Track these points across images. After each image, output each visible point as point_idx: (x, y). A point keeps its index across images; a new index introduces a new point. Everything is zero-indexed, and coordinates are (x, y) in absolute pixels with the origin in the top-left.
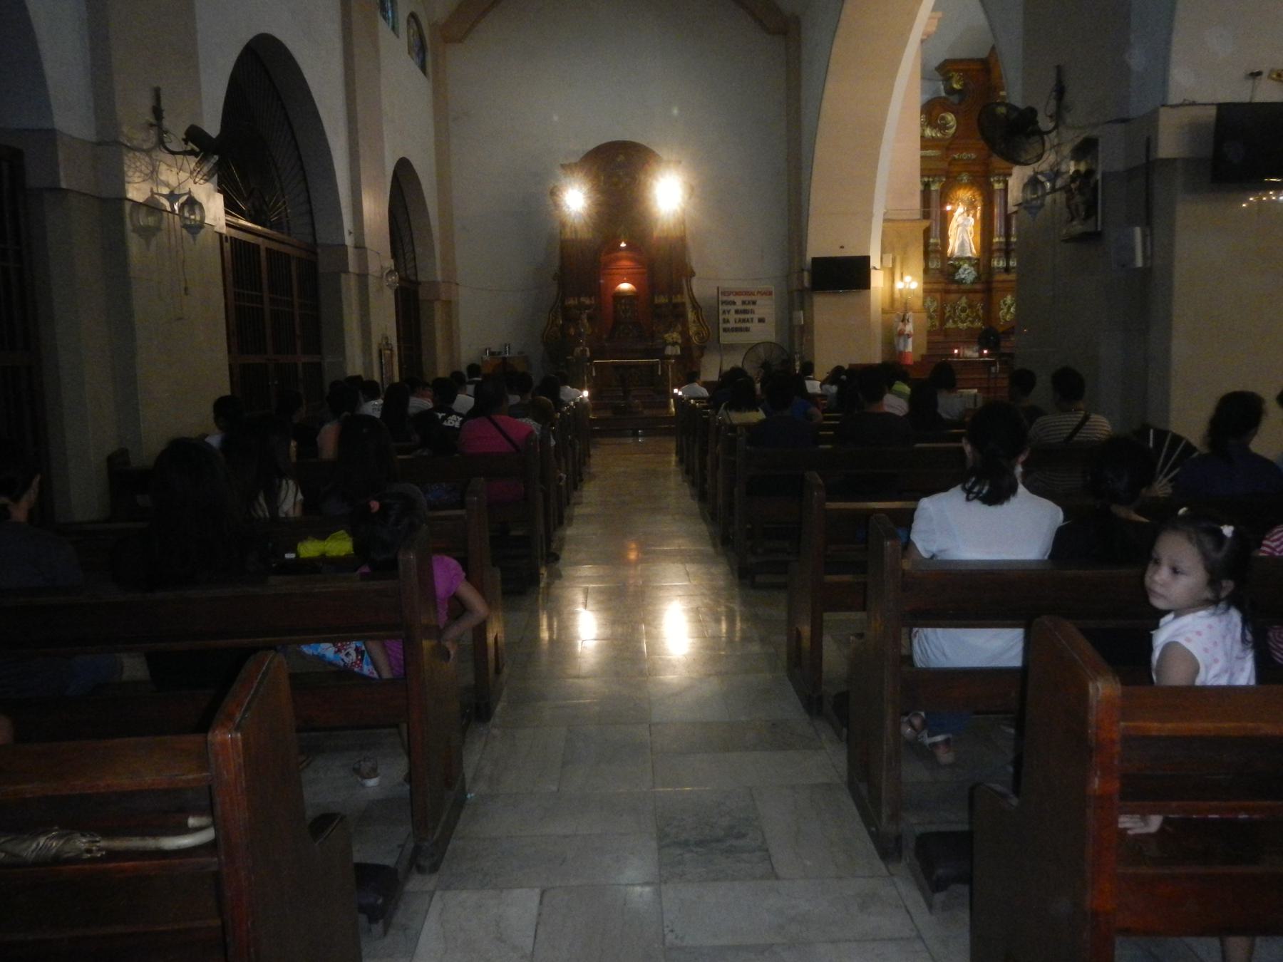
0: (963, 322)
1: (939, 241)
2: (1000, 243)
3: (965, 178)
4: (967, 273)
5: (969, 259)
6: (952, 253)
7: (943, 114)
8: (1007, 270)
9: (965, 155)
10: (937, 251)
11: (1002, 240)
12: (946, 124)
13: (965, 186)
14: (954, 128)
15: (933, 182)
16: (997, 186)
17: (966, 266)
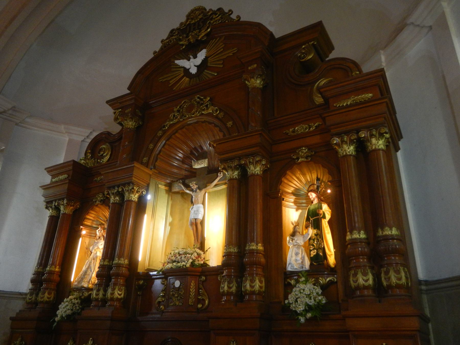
10: (48, 281)
12: (103, 154)
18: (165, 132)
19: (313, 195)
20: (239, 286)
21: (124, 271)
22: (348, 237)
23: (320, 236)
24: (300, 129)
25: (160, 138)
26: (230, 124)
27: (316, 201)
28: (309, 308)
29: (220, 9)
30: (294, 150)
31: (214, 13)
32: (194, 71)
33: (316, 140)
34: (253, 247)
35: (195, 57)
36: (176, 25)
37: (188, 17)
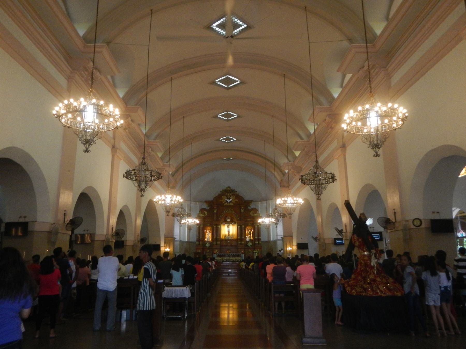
0: (208, 255)
1: (202, 238)
2: (215, 238)
3: (208, 225)
4: (208, 245)
5: (209, 242)
6: (206, 240)
7: (204, 212)
8: (217, 244)
9: (208, 220)
11: (215, 238)
13: (208, 226)
14: (207, 214)
15: (201, 225)
16: (215, 227)
17: (208, 243)
18: (223, 214)
19: (250, 230)
20: (241, 243)
21: (219, 239)
22: (255, 237)
23: (251, 236)
24: (249, 220)
25: (222, 215)
26: (237, 216)
27: (250, 231)
28: (251, 246)
29: (234, 190)
30: (248, 223)
31: (233, 190)
32: (229, 202)
33: (251, 222)
34: (243, 237)
35: (230, 199)
36: (224, 189)
37: (227, 188)
